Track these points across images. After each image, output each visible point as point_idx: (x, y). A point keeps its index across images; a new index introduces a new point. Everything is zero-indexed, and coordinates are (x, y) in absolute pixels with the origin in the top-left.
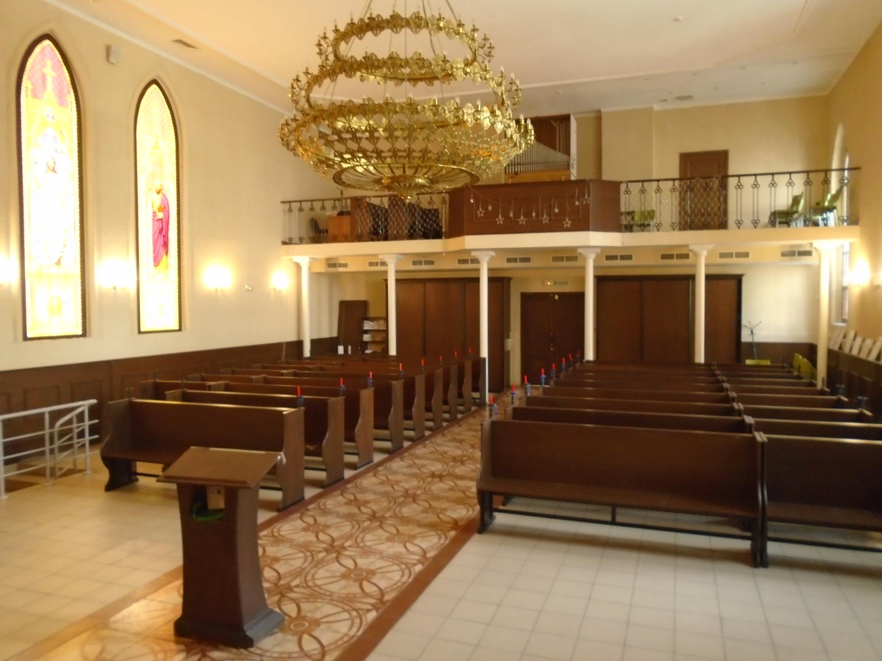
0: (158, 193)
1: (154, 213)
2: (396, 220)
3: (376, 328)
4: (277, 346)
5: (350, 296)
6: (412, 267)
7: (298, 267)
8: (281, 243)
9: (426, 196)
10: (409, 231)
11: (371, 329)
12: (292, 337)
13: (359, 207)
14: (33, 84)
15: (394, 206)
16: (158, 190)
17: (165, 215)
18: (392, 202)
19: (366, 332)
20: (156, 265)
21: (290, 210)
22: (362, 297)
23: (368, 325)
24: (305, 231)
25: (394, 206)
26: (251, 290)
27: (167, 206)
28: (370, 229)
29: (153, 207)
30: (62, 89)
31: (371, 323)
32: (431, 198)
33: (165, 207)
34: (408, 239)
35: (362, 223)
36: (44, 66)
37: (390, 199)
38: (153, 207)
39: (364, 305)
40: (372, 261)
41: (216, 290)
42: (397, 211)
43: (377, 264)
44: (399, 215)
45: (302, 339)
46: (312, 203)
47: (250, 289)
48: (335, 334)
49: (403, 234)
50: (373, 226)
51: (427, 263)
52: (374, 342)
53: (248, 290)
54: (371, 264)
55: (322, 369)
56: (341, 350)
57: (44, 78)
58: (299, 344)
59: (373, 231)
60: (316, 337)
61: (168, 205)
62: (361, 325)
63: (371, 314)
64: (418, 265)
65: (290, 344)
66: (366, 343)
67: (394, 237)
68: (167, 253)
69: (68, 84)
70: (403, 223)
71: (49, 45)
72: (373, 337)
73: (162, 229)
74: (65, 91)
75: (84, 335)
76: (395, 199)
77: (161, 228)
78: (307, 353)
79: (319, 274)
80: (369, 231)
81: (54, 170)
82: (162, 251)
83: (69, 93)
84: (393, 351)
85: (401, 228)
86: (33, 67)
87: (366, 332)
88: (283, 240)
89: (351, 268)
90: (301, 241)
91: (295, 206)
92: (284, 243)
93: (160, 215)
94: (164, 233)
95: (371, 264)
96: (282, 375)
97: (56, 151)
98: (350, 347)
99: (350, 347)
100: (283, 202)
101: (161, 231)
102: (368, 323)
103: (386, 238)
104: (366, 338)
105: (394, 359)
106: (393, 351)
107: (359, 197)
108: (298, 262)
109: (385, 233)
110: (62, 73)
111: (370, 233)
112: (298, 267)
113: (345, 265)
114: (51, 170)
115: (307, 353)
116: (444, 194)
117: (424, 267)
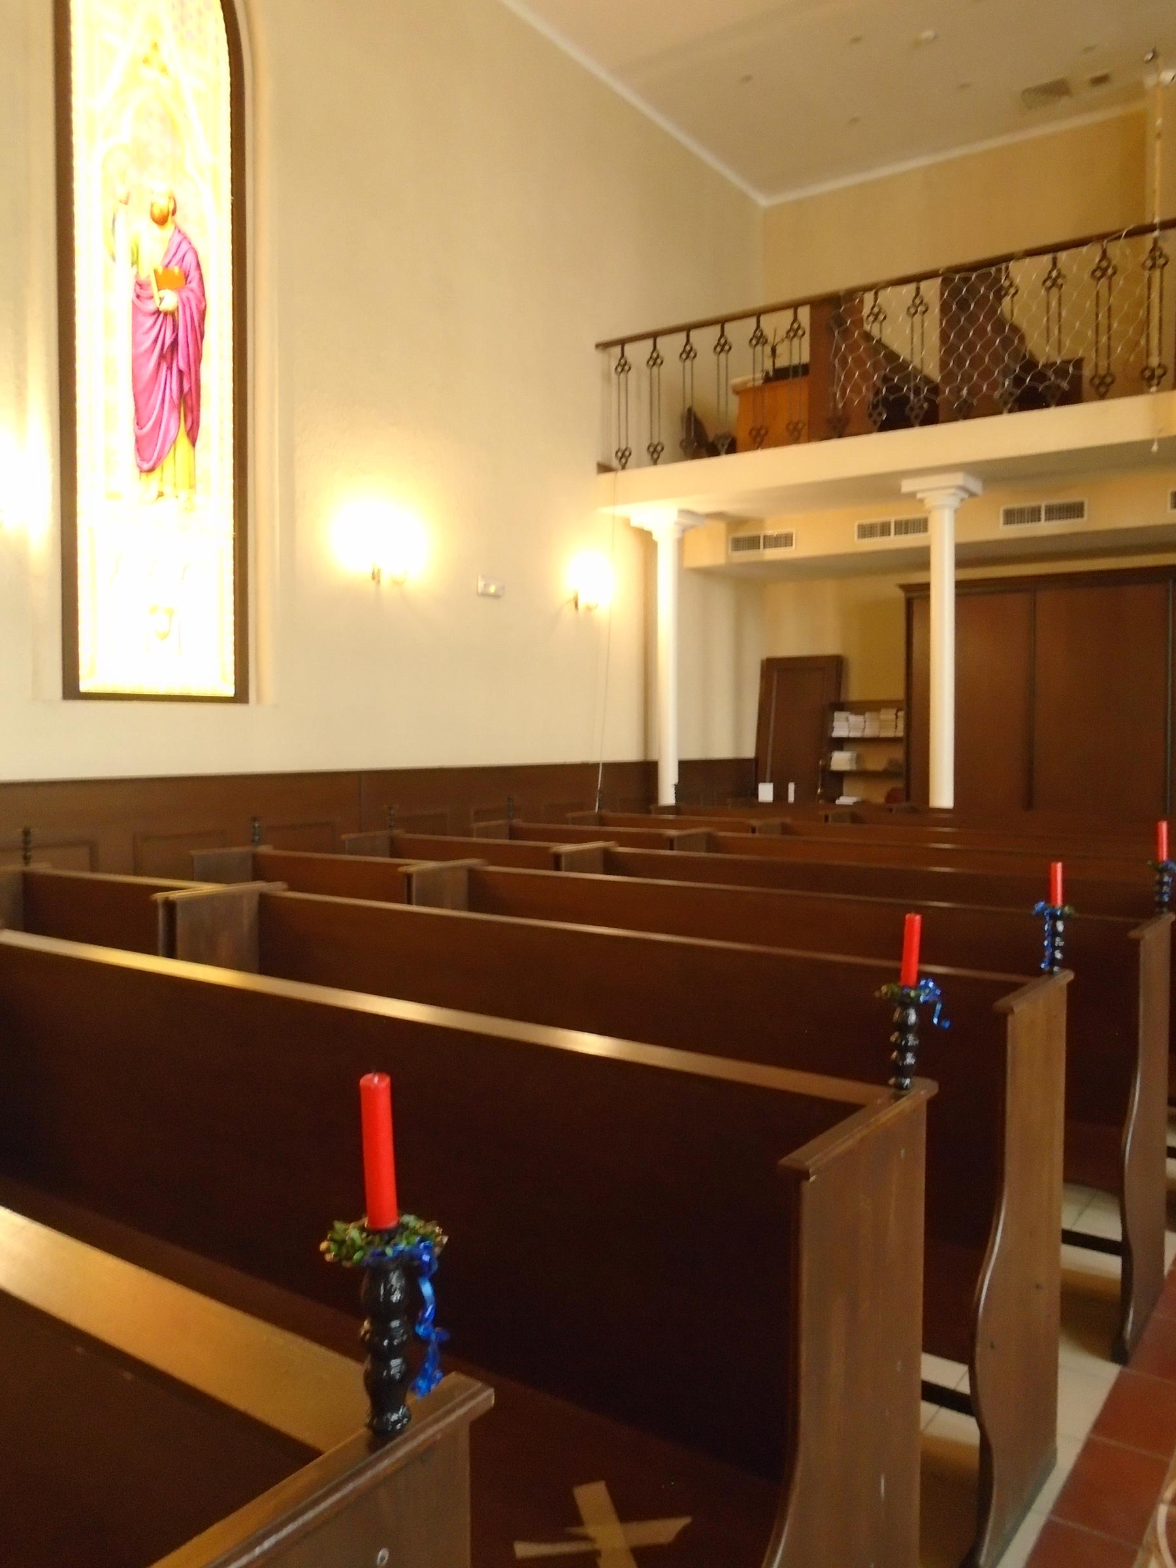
0: (161, 221)
1: (140, 285)
2: (970, 348)
3: (869, 732)
4: (582, 772)
5: (791, 646)
6: (997, 530)
7: (646, 541)
8: (593, 468)
9: (1085, 249)
10: (1018, 381)
11: (852, 735)
12: (626, 751)
13: (840, 321)
15: (963, 305)
16: (157, 212)
17: (185, 303)
18: (955, 292)
19: (841, 744)
20: (146, 466)
21: (623, 366)
22: (828, 646)
23: (844, 726)
24: (670, 434)
25: (963, 305)
26: (496, 596)
27: (194, 274)
28: (877, 392)
29: (135, 263)
31: (854, 719)
32: (1104, 254)
34: (1011, 411)
35: (849, 376)
37: (946, 281)
38: (135, 263)
39: (833, 668)
40: (867, 521)
41: (375, 577)
42: (972, 319)
43: (884, 530)
44: (980, 332)
45: (653, 757)
46: (688, 336)
47: (492, 589)
48: (748, 751)
49: (997, 394)
50: (886, 379)
51: (1055, 512)
52: (860, 775)
53: (485, 595)
54: (866, 531)
55: (713, 843)
56: (766, 792)
58: (647, 771)
59: (885, 399)
60: (694, 754)
62: (826, 724)
63: (855, 691)
64: (1021, 521)
65: (615, 769)
66: (840, 776)
67: (960, 408)
68: (192, 435)
70: (997, 359)
72: (859, 759)
73: (175, 343)
76: (966, 280)
77: (168, 340)
78: (668, 796)
79: (707, 573)
80: (871, 396)
84: (943, 794)
85: (986, 374)
87: (841, 744)
88: (600, 459)
89: (804, 548)
90: (655, 454)
91: (638, 353)
92: (604, 468)
93: (169, 300)
94: (181, 362)
95: (866, 531)
96: (556, 862)
98: (792, 787)
99: (792, 787)
100: (604, 346)
102: (847, 720)
103: (931, 418)
104: (841, 760)
105: (947, 816)
106: (943, 794)
107: (841, 294)
108: (646, 528)
109: (926, 399)
111: (875, 407)
112: (646, 541)
113: (785, 540)
115: (668, 796)
116: (1156, 233)
117: (1045, 528)
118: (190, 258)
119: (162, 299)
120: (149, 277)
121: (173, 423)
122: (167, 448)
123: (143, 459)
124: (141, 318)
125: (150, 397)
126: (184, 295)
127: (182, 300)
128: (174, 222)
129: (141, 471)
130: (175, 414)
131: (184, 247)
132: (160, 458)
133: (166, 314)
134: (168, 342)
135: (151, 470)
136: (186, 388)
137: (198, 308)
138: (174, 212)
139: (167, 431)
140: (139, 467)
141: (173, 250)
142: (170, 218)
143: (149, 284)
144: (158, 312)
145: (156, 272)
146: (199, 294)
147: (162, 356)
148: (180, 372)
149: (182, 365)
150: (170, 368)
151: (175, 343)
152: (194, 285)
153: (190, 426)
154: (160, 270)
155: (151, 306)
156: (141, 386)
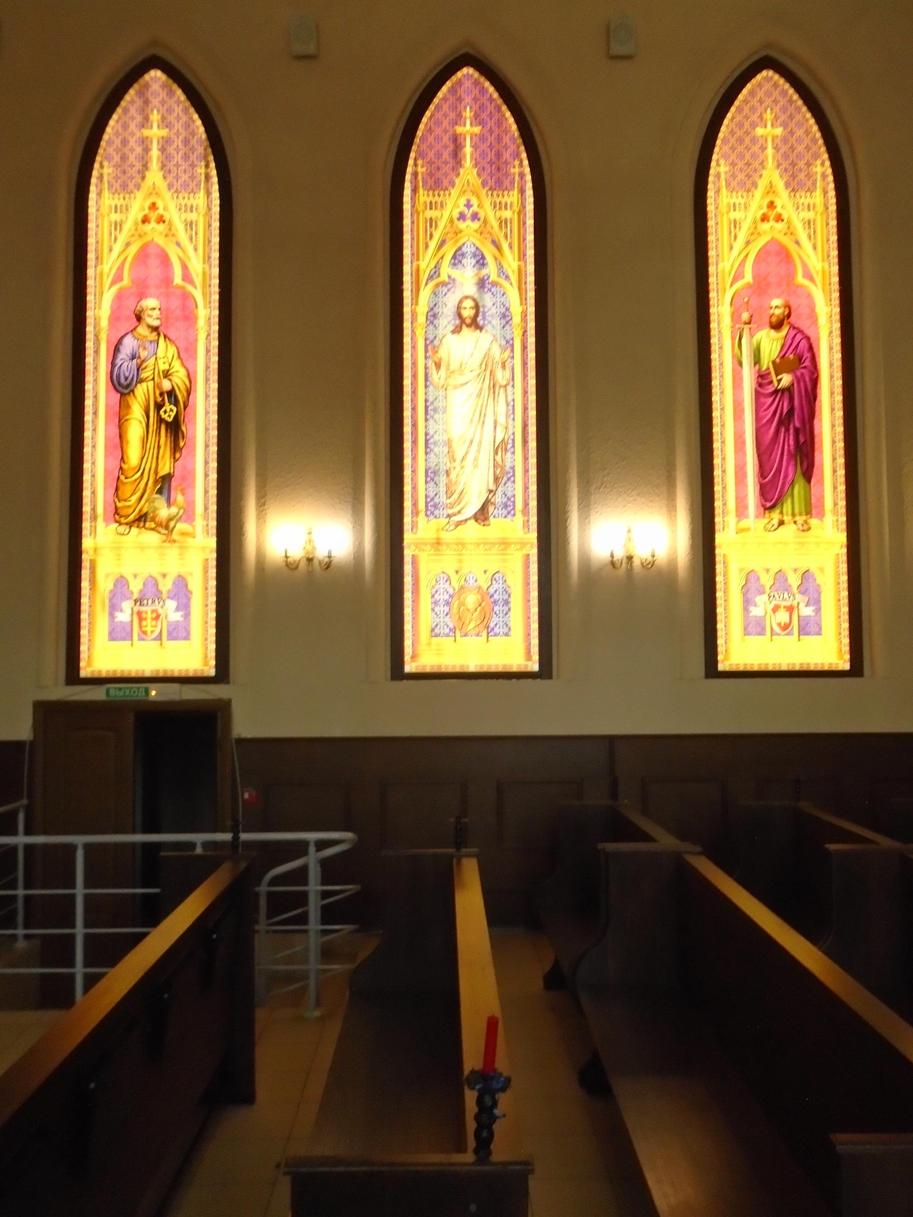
14: (431, 163)
16: (774, 319)
17: (798, 379)
20: (769, 504)
30: (499, 155)
33: (800, 358)
36: (458, 119)
57: (457, 143)
61: (811, 348)
68: (808, 475)
69: (513, 138)
71: (468, 76)
73: (791, 410)
74: (507, 155)
75: (546, 670)
81: (475, 324)
82: (794, 472)
83: (517, 155)
86: (430, 130)
93: (786, 379)
97: (482, 283)
101: (785, 421)
110: (499, 123)
114: (468, 326)
118: (804, 342)
119: (779, 381)
120: (768, 369)
121: (791, 469)
122: (786, 488)
123: (766, 500)
124: (763, 400)
125: (771, 454)
126: (798, 373)
127: (796, 377)
128: (789, 323)
129: (765, 509)
130: (792, 463)
131: (799, 337)
132: (780, 497)
133: (783, 390)
134: (785, 411)
135: (772, 507)
136: (802, 440)
137: (811, 379)
138: (789, 315)
139: (786, 477)
140: (763, 506)
141: (789, 342)
142: (785, 321)
143: (769, 374)
144: (776, 392)
145: (774, 362)
146: (812, 369)
147: (780, 423)
148: (797, 431)
149: (797, 424)
150: (787, 430)
151: (791, 410)
152: (807, 363)
153: (805, 468)
154: (778, 360)
155: (771, 389)
156: (763, 448)
